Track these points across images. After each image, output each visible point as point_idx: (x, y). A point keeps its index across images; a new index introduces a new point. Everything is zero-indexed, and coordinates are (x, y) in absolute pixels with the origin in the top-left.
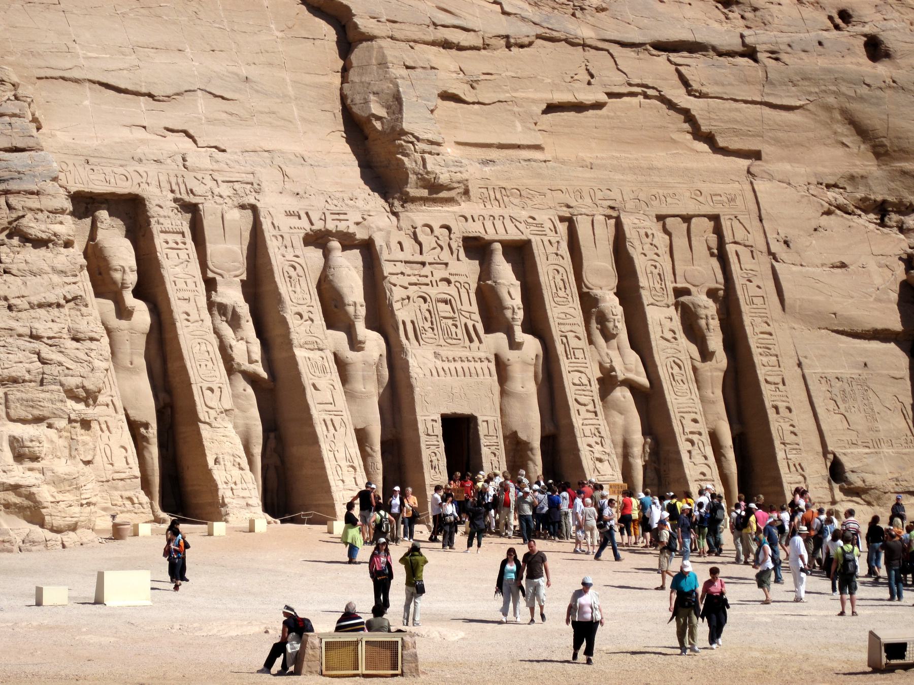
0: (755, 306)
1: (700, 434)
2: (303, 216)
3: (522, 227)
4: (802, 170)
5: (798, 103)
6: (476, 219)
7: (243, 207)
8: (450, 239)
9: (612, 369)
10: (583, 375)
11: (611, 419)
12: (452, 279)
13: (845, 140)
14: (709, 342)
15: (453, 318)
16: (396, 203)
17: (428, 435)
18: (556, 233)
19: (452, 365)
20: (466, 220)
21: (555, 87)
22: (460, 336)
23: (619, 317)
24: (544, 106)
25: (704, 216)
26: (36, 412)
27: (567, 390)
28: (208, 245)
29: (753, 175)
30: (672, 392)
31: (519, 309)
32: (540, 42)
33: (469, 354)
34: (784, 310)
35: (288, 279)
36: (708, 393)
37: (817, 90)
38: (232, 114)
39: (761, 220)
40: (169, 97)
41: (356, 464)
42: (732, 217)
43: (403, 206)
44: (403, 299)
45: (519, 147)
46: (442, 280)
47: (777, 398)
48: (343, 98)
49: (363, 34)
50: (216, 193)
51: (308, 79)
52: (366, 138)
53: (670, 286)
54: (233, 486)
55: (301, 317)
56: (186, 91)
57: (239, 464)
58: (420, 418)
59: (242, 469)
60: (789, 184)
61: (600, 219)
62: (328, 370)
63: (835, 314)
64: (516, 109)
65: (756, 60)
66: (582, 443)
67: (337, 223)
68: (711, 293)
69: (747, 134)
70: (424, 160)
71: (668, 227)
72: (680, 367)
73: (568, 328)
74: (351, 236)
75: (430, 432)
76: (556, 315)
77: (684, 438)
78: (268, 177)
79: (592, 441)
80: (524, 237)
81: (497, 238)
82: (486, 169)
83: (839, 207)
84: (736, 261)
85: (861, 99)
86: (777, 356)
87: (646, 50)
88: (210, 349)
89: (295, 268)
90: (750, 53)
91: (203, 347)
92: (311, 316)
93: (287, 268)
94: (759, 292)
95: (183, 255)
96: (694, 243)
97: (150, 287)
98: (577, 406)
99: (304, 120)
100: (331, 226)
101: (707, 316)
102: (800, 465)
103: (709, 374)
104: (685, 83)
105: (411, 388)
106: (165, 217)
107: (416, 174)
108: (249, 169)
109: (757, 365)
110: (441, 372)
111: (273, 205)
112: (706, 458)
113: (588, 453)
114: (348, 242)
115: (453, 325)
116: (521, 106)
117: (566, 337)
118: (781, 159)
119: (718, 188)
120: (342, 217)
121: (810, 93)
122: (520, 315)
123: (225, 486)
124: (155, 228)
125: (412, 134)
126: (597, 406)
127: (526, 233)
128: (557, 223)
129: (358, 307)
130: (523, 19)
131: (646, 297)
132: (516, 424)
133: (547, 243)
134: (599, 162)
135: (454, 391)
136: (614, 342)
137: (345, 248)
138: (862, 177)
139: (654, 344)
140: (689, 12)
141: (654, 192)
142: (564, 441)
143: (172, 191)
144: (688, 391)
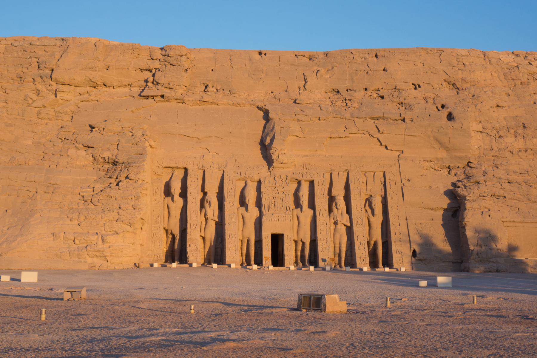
2: (239, 173)
5: (418, 135)
7: (220, 170)
26: (113, 229)
48: (262, 137)
65: (404, 122)
97: (184, 194)
100: (247, 176)
107: (277, 160)
132: (301, 236)
136: (340, 211)
139: (352, 212)
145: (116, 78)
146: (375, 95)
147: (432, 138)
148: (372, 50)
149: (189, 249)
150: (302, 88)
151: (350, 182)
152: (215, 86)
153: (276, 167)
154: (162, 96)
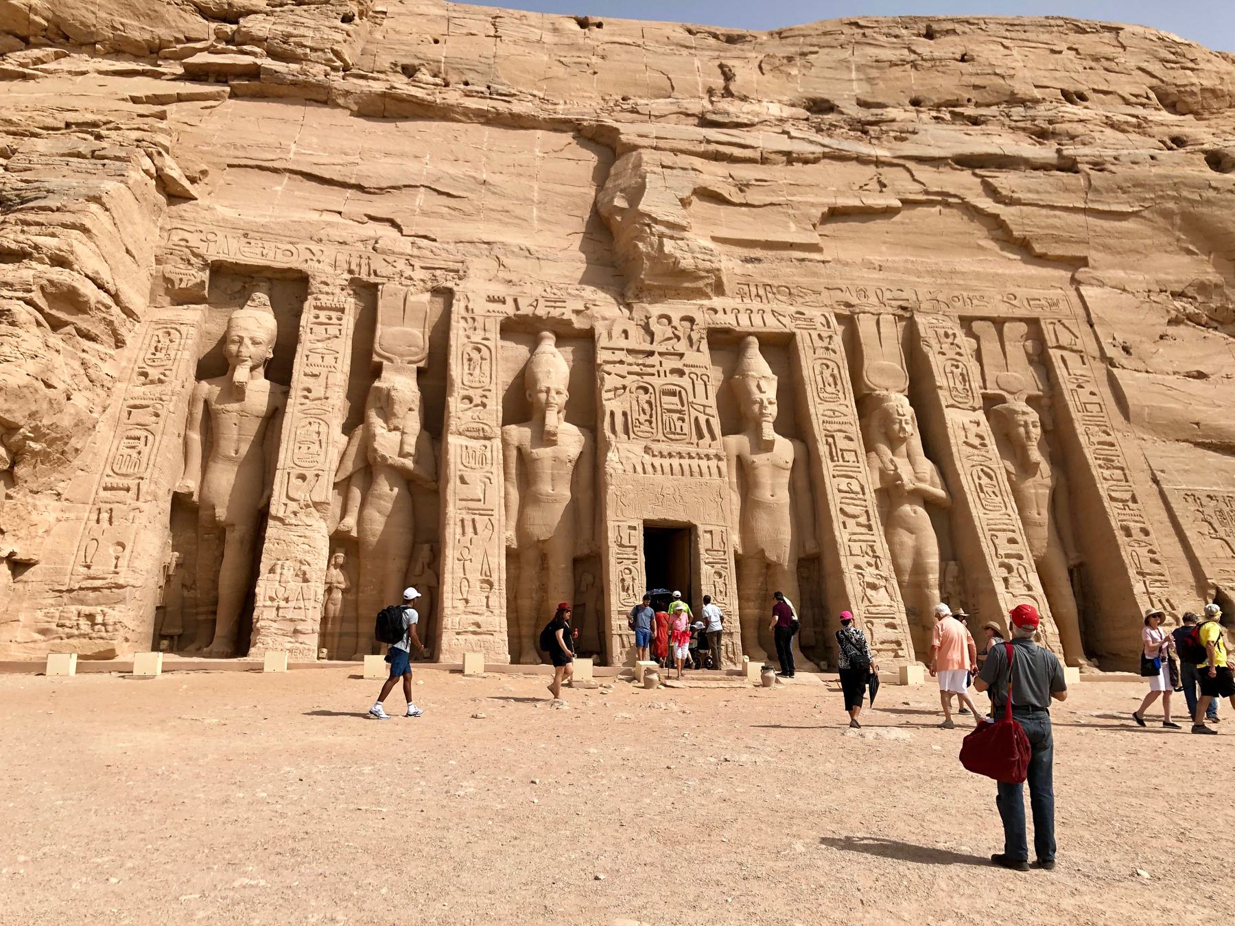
1: (1020, 557)
2: (510, 301)
3: (786, 321)
4: (1141, 278)
5: (1130, 210)
6: (728, 311)
7: (436, 291)
8: (692, 330)
9: (899, 478)
10: (853, 481)
11: (896, 539)
12: (687, 370)
13: (1191, 247)
15: (680, 412)
16: (630, 294)
17: (621, 545)
18: (829, 327)
19: (666, 462)
20: (716, 312)
21: (839, 193)
22: (686, 430)
23: (908, 417)
24: (826, 209)
25: (1021, 320)
27: (830, 497)
28: (379, 326)
29: (1079, 283)
30: (979, 506)
31: (770, 403)
32: (827, 161)
33: (693, 450)
34: (1127, 417)
35: (465, 361)
36: (1033, 514)
37: (1152, 196)
38: (455, 209)
39: (1092, 326)
40: (381, 189)
41: (495, 578)
43: (637, 297)
44: (616, 389)
45: (791, 246)
46: (673, 371)
48: (595, 204)
49: (624, 144)
50: (405, 275)
51: (559, 188)
52: (613, 239)
53: (978, 392)
54: (283, 604)
55: (471, 401)
56: (405, 186)
57: (304, 573)
58: (611, 524)
59: (306, 580)
60: (1124, 290)
61: (887, 319)
62: (489, 461)
63: (1197, 424)
64: (791, 211)
65: (1077, 172)
66: (847, 564)
67: (551, 310)
68: (1030, 401)
69: (1069, 241)
70: (661, 245)
72: (991, 478)
73: (837, 427)
74: (569, 323)
75: (625, 542)
76: (820, 412)
77: (997, 562)
78: (479, 267)
79: (862, 561)
80: (787, 330)
81: (752, 330)
82: (749, 265)
83: (1190, 318)
84: (1062, 365)
85: (1209, 202)
86: (1122, 469)
87: (948, 164)
88: (323, 428)
89: (479, 350)
90: (1068, 165)
91: (315, 427)
92: (484, 400)
93: (469, 349)
94: (1094, 399)
95: (333, 330)
96: (1008, 347)
98: (842, 518)
99: (541, 219)
100: (541, 311)
101: (1026, 422)
104: (992, 192)
105: (606, 485)
106: (327, 293)
108: (459, 257)
110: (649, 469)
111: (478, 292)
113: (855, 576)
114: (565, 334)
115: (679, 419)
116: (798, 209)
117: (833, 437)
118: (1113, 266)
119: (1035, 293)
120: (558, 304)
121: (1144, 200)
122: (772, 410)
123: (268, 603)
124: (309, 303)
125: (649, 216)
126: (872, 518)
127: (789, 326)
128: (833, 321)
129: (553, 393)
130: (811, 142)
131: (944, 398)
133: (815, 336)
134: (889, 264)
135: (665, 492)
136: (903, 448)
137: (561, 340)
138: (1216, 286)
139: (954, 449)
140: (997, 140)
141: (956, 294)
142: (827, 561)
143: (350, 272)
145: (103, 15)
146: (948, 117)
147: (1178, 221)
148: (915, 20)
149: (264, 588)
150: (719, 92)
151: (925, 349)
152: (443, 75)
153: (650, 289)
154: (253, 73)
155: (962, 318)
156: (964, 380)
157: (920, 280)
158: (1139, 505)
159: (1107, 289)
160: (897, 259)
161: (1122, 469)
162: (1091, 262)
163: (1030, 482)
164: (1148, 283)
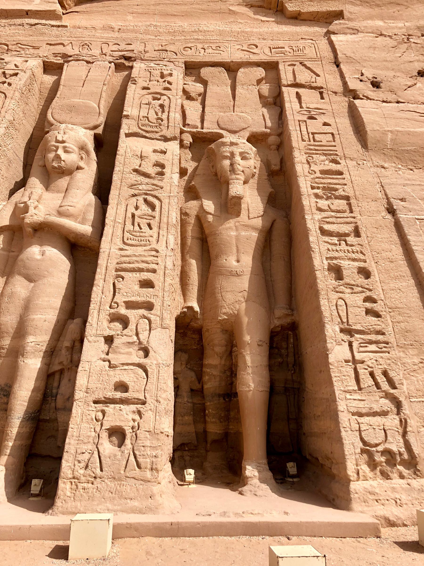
0: (316, 143)
4: (401, 25)
14: (230, 186)
25: (258, 64)
39: (338, 66)
42: (298, 63)
45: (27, 14)
47: (341, 254)
68: (254, 139)
71: (202, 75)
72: (153, 207)
84: (295, 100)
94: (327, 129)
96: (239, 90)
101: (233, 154)
102: (385, 373)
103: (233, 233)
109: (307, 208)
112: (146, 352)
118: (371, 18)
119: (281, 43)
141: (190, 45)
144: (153, 240)
155: (186, 63)
156: (163, 111)
157: (159, 37)
158: (363, 239)
159: (361, 35)
160: (140, 24)
161: (347, 198)
162: (346, 14)
163: (231, 223)
164: (408, 28)
